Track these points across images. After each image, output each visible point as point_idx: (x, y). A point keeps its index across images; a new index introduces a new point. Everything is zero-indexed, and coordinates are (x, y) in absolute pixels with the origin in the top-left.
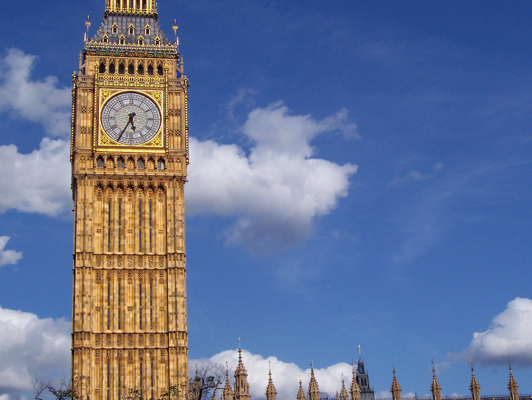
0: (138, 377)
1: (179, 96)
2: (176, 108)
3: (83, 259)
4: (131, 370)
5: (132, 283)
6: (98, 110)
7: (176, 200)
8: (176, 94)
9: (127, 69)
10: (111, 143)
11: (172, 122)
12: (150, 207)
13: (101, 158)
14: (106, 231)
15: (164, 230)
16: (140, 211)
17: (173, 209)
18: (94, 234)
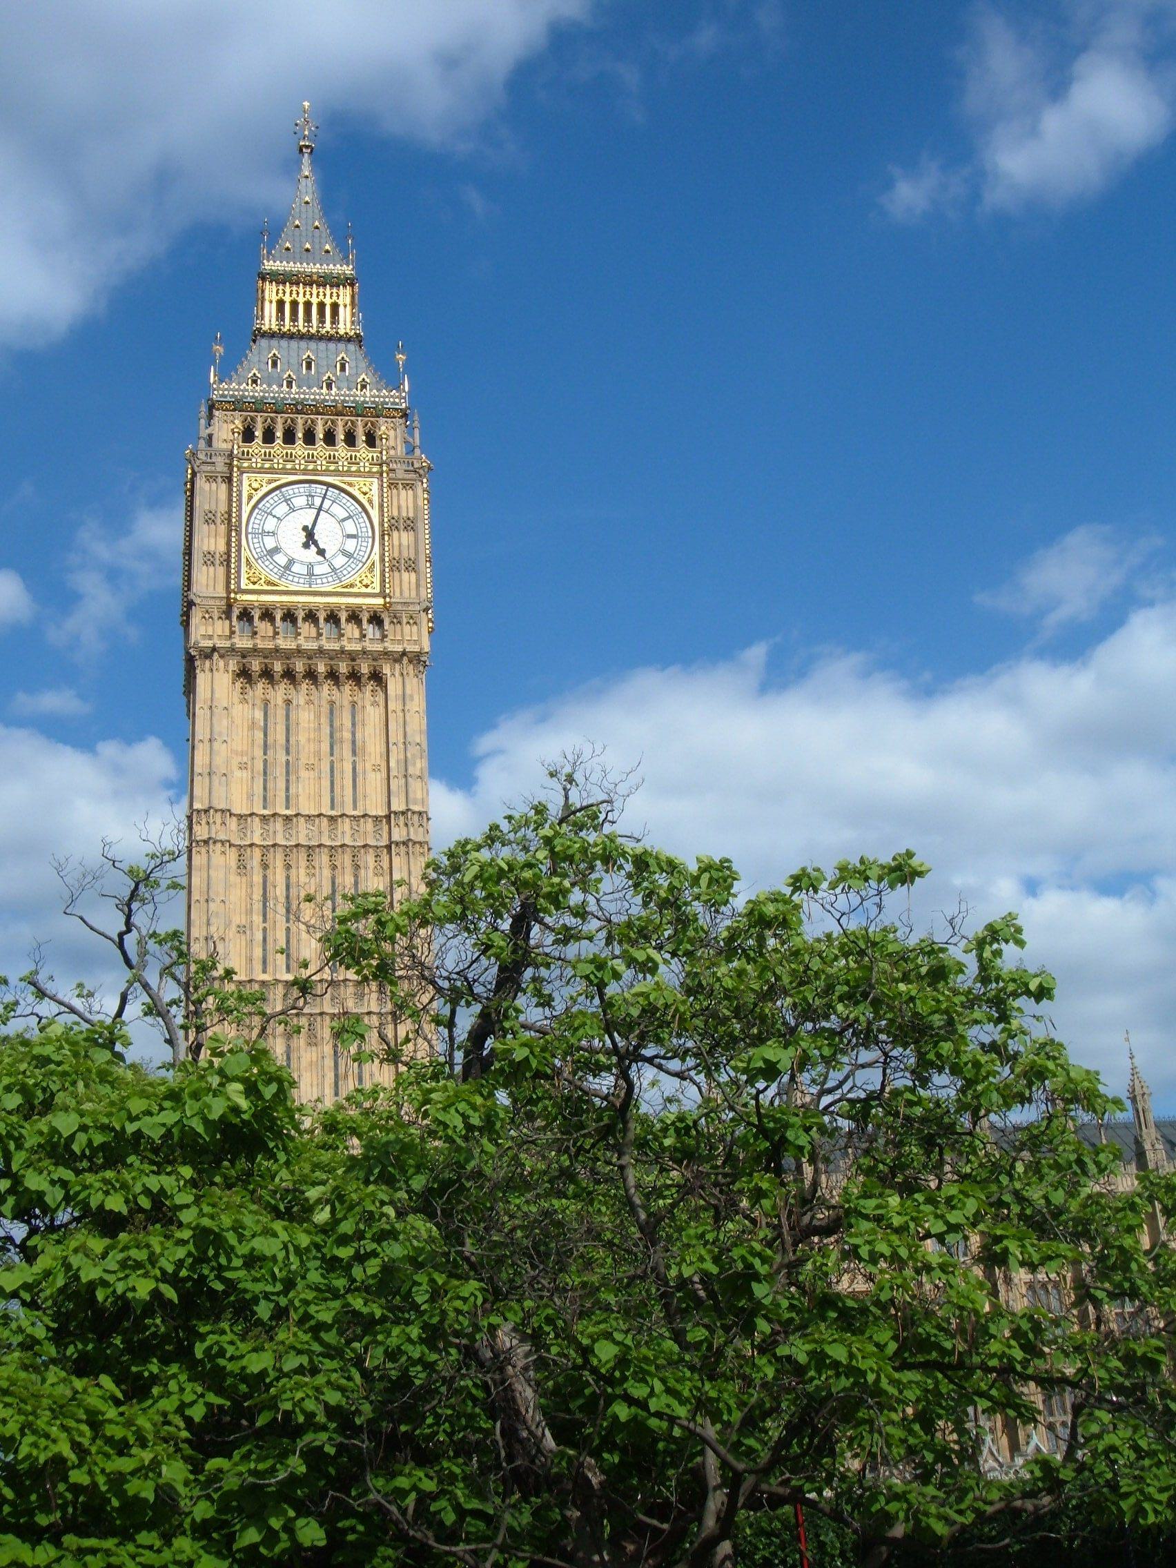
0: (330, 1076)
1: (410, 492)
2: (404, 514)
3: (208, 823)
4: (314, 1059)
5: (314, 875)
6: (239, 516)
7: (408, 702)
8: (405, 486)
9: (300, 435)
10: (269, 583)
11: (396, 543)
12: (353, 717)
13: (246, 615)
14: (259, 766)
15: (384, 764)
16: (331, 726)
17: (401, 720)
18: (232, 772)
